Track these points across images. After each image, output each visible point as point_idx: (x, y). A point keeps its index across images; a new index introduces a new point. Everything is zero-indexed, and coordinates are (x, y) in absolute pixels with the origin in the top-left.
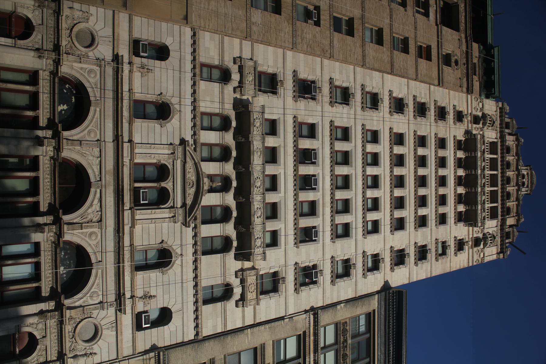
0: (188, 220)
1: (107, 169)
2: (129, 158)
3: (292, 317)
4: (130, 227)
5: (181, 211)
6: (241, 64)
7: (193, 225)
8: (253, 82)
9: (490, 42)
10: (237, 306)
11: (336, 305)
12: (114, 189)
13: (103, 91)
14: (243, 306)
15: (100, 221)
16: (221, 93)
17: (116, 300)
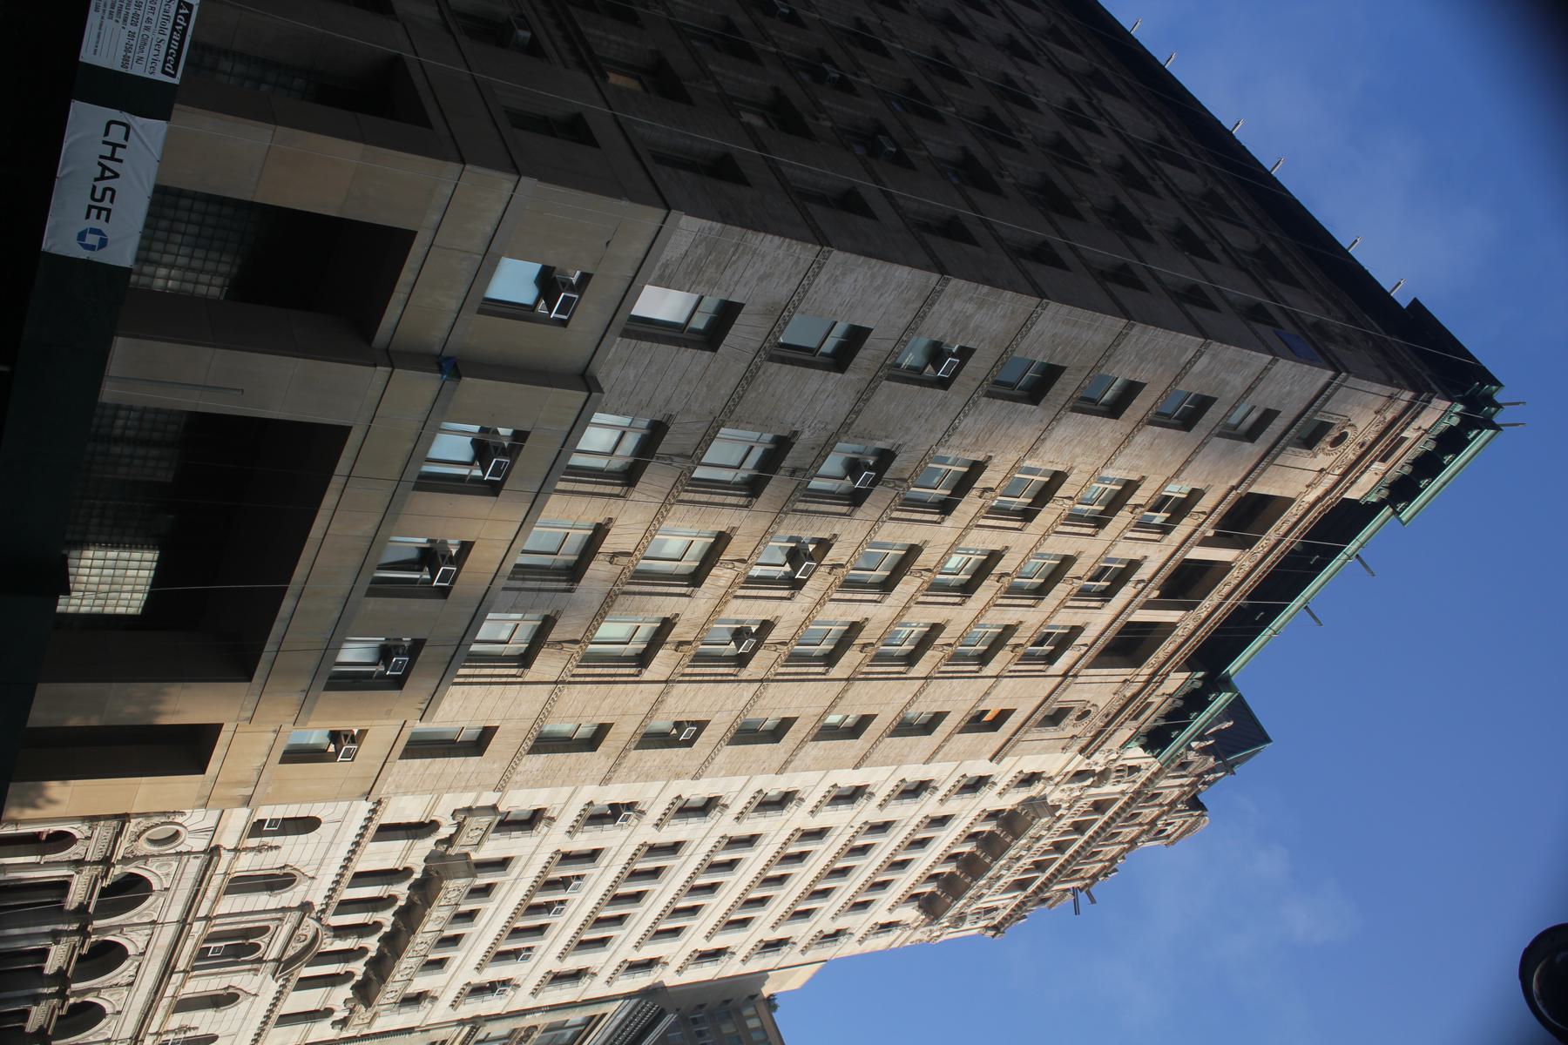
0: (277, 976)
1: (157, 944)
2: (200, 933)
3: (429, 1030)
4: (177, 988)
5: (272, 965)
6: (463, 821)
7: (281, 982)
8: (479, 838)
9: (1231, 672)
10: (334, 1024)
11: (526, 1014)
12: (163, 961)
13: (177, 881)
14: (341, 1029)
15: (131, 984)
16: (406, 849)
17: (131, 1038)
